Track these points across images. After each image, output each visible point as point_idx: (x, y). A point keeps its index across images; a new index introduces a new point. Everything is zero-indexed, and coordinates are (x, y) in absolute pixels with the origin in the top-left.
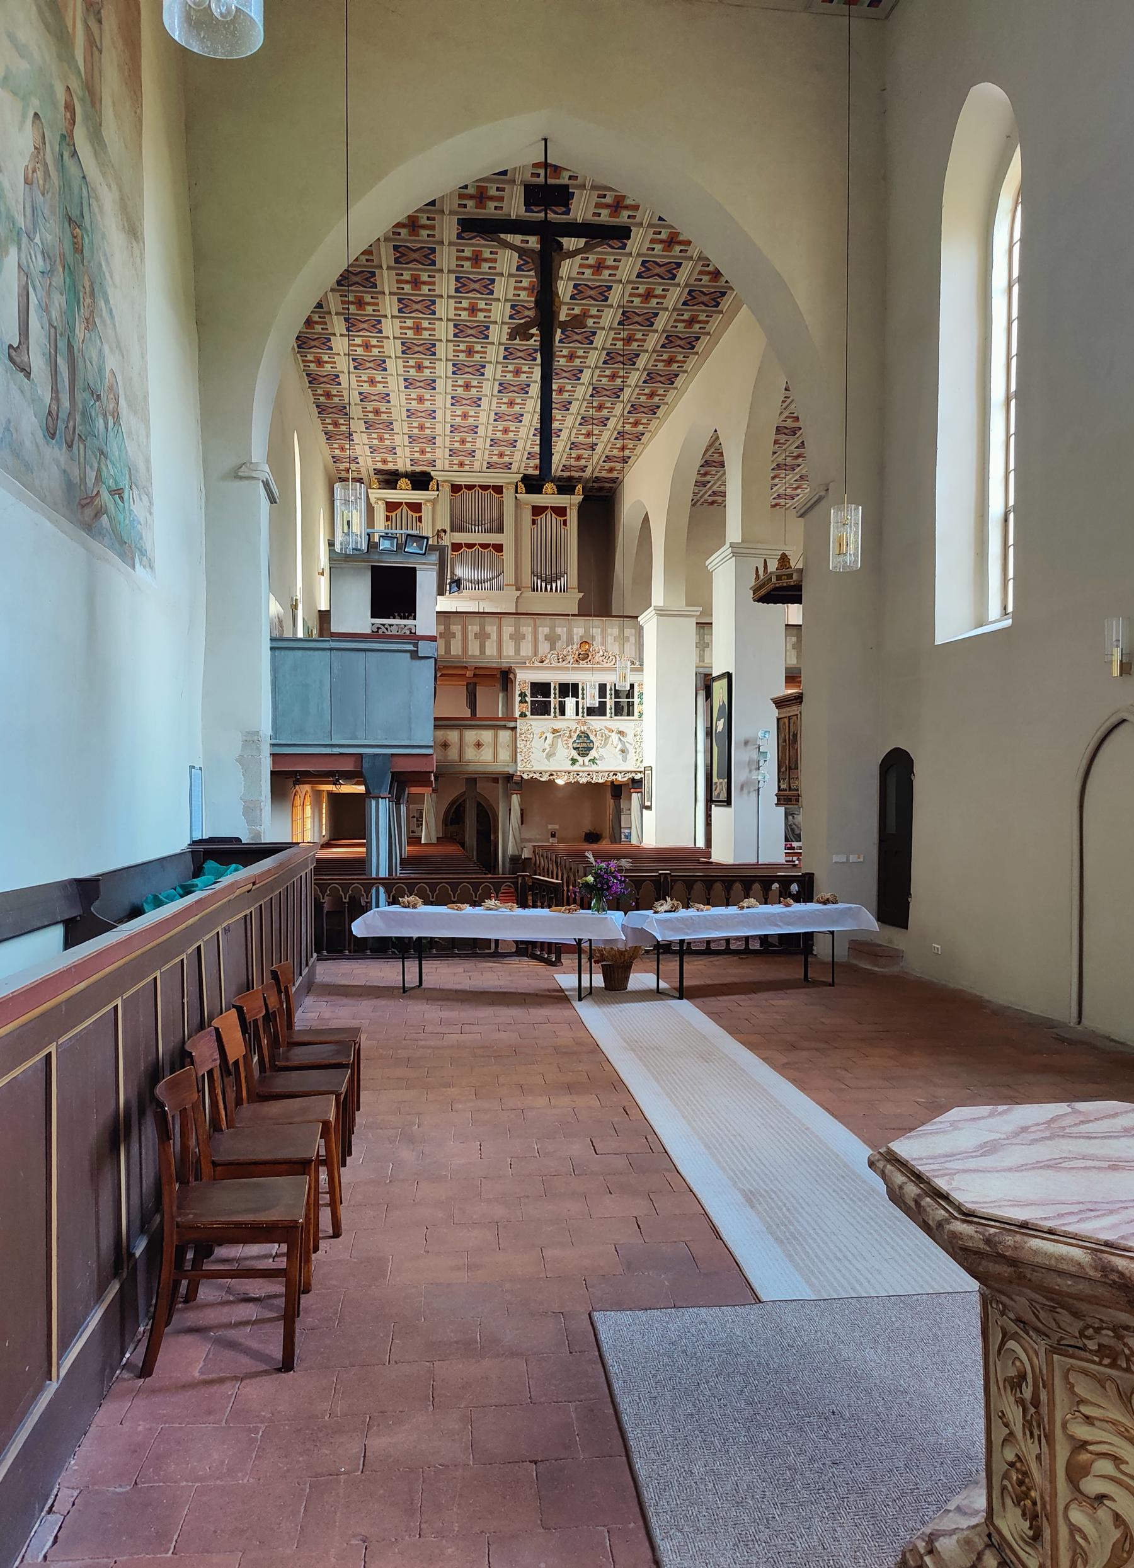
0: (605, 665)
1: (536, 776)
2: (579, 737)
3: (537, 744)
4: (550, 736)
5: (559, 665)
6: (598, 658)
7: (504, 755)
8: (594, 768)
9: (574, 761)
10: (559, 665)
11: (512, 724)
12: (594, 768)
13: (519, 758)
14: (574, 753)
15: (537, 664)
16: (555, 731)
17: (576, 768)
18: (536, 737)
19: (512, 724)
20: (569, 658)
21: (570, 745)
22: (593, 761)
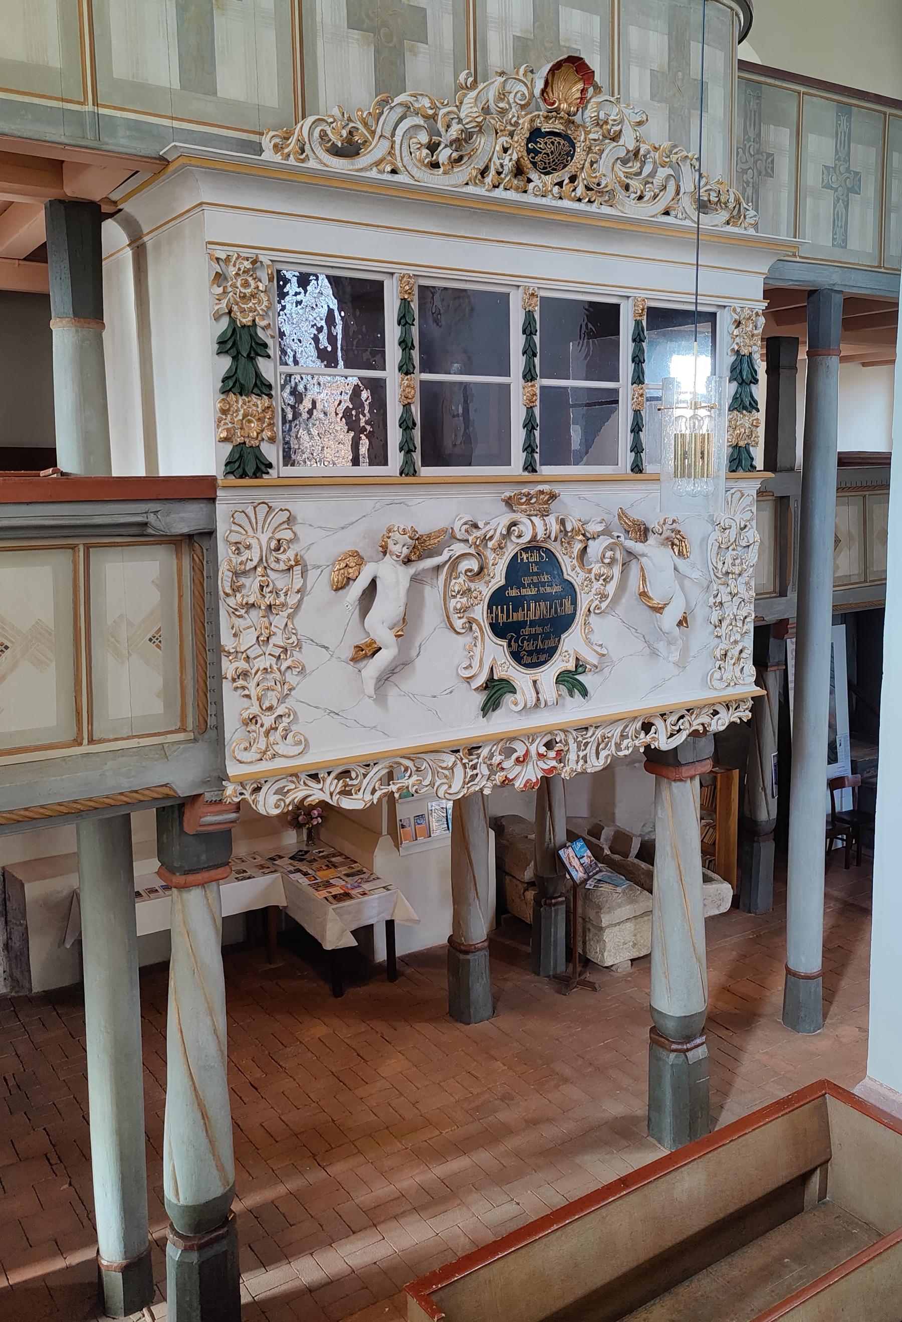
0: (630, 208)
1: (322, 792)
2: (515, 570)
3: (325, 619)
4: (393, 579)
5: (436, 180)
6: (607, 170)
7: (136, 688)
8: (575, 711)
9: (495, 691)
10: (436, 180)
11: (184, 518)
12: (575, 711)
13: (234, 707)
14: (495, 654)
15: (322, 161)
16: (421, 547)
17: (503, 722)
18: (319, 584)
19: (184, 518)
20: (485, 146)
21: (480, 613)
22: (571, 682)
